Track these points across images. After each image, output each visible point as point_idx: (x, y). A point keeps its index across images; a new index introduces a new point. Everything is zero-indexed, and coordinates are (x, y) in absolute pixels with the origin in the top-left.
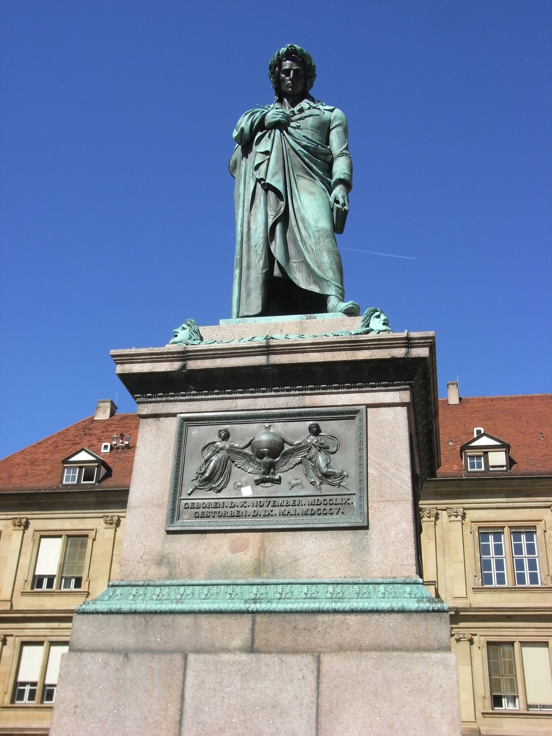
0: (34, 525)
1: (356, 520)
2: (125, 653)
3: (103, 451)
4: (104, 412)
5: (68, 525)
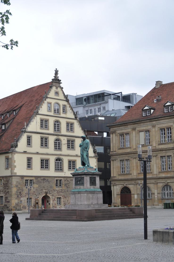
0: (137, 129)
1: (83, 185)
2: (73, 194)
3: (155, 102)
4: (158, 85)
5: (144, 128)
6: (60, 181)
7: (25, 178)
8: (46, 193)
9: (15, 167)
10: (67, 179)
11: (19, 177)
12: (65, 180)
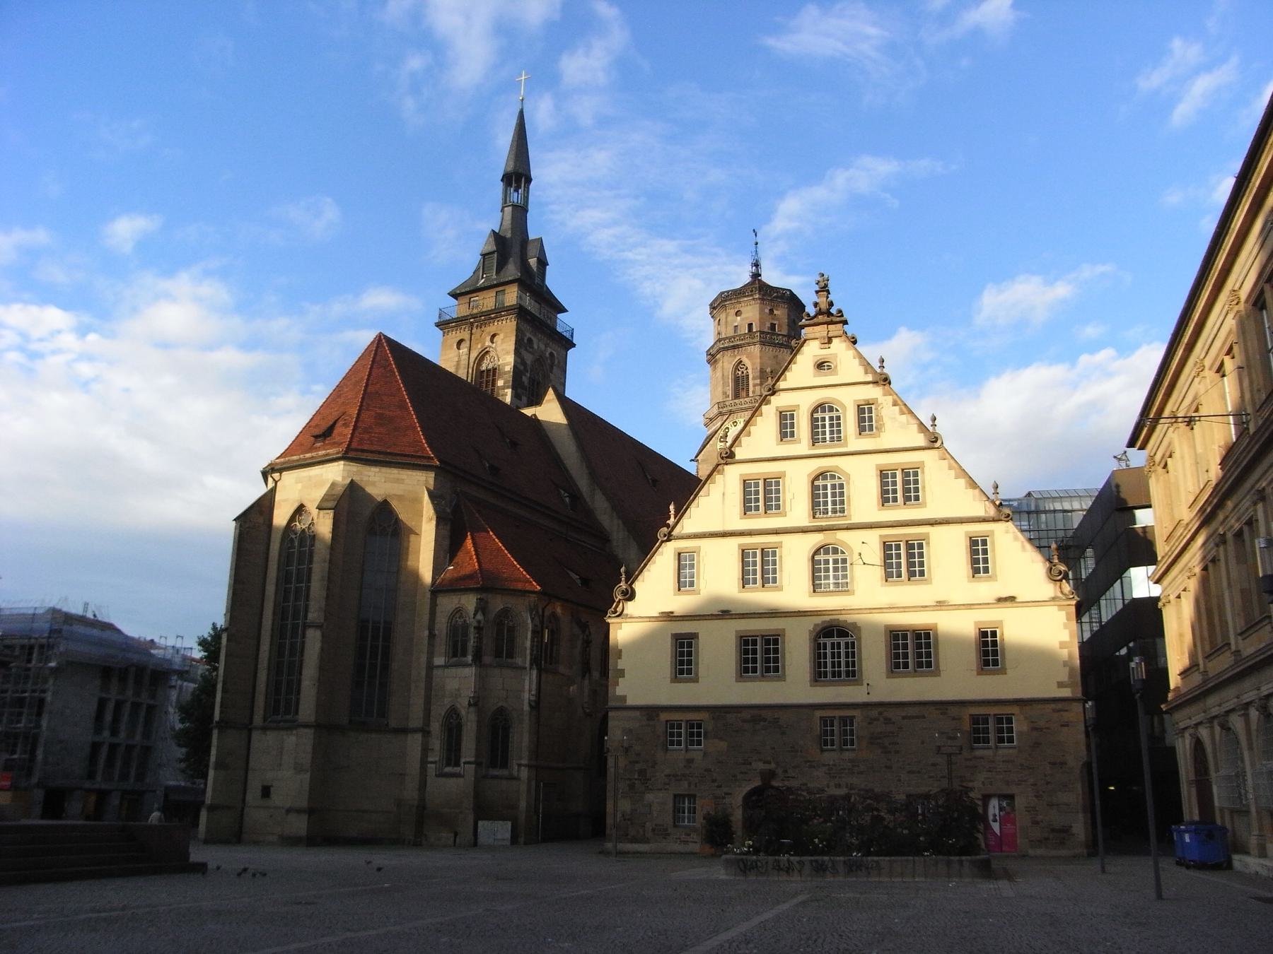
6: (846, 721)
7: (664, 716)
8: (768, 776)
9: (621, 673)
10: (880, 713)
11: (638, 713)
12: (872, 721)
